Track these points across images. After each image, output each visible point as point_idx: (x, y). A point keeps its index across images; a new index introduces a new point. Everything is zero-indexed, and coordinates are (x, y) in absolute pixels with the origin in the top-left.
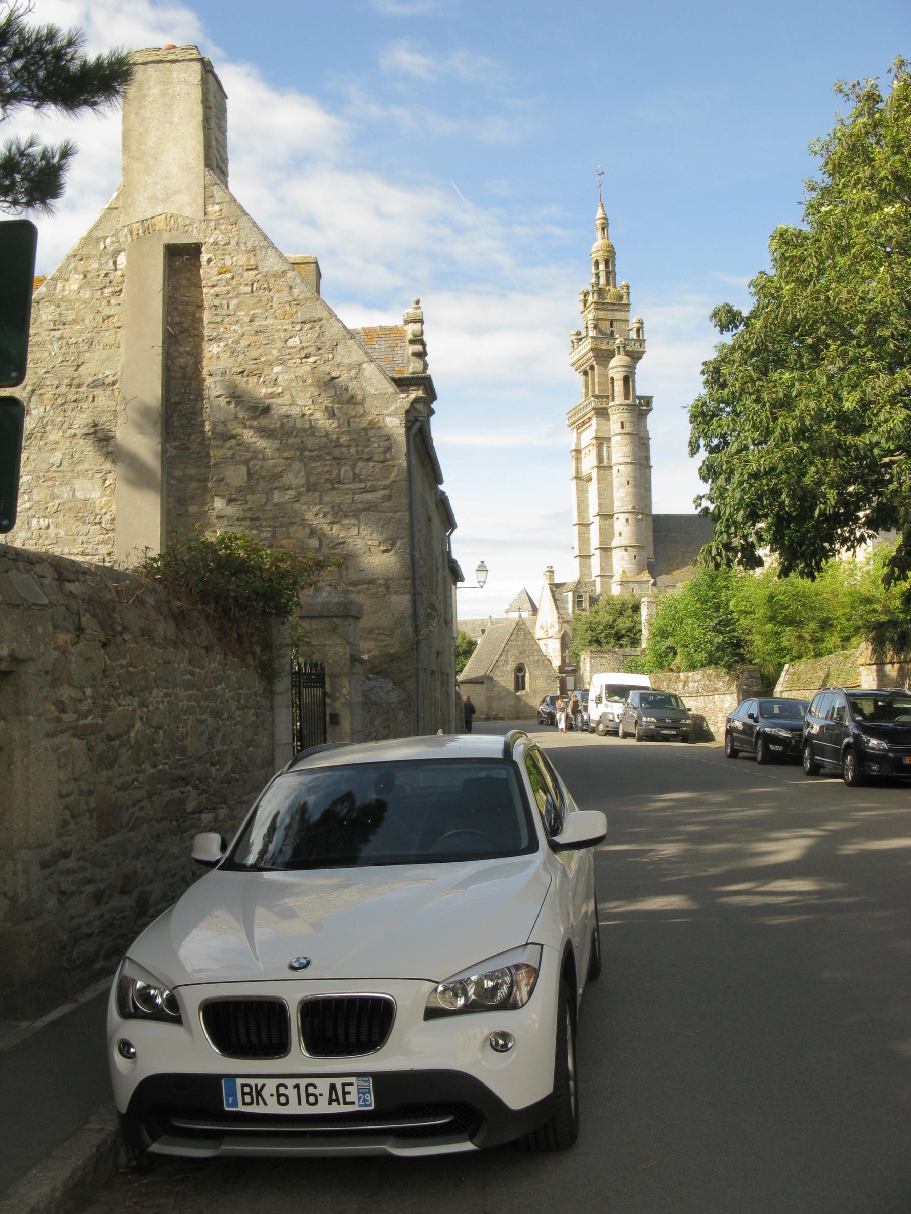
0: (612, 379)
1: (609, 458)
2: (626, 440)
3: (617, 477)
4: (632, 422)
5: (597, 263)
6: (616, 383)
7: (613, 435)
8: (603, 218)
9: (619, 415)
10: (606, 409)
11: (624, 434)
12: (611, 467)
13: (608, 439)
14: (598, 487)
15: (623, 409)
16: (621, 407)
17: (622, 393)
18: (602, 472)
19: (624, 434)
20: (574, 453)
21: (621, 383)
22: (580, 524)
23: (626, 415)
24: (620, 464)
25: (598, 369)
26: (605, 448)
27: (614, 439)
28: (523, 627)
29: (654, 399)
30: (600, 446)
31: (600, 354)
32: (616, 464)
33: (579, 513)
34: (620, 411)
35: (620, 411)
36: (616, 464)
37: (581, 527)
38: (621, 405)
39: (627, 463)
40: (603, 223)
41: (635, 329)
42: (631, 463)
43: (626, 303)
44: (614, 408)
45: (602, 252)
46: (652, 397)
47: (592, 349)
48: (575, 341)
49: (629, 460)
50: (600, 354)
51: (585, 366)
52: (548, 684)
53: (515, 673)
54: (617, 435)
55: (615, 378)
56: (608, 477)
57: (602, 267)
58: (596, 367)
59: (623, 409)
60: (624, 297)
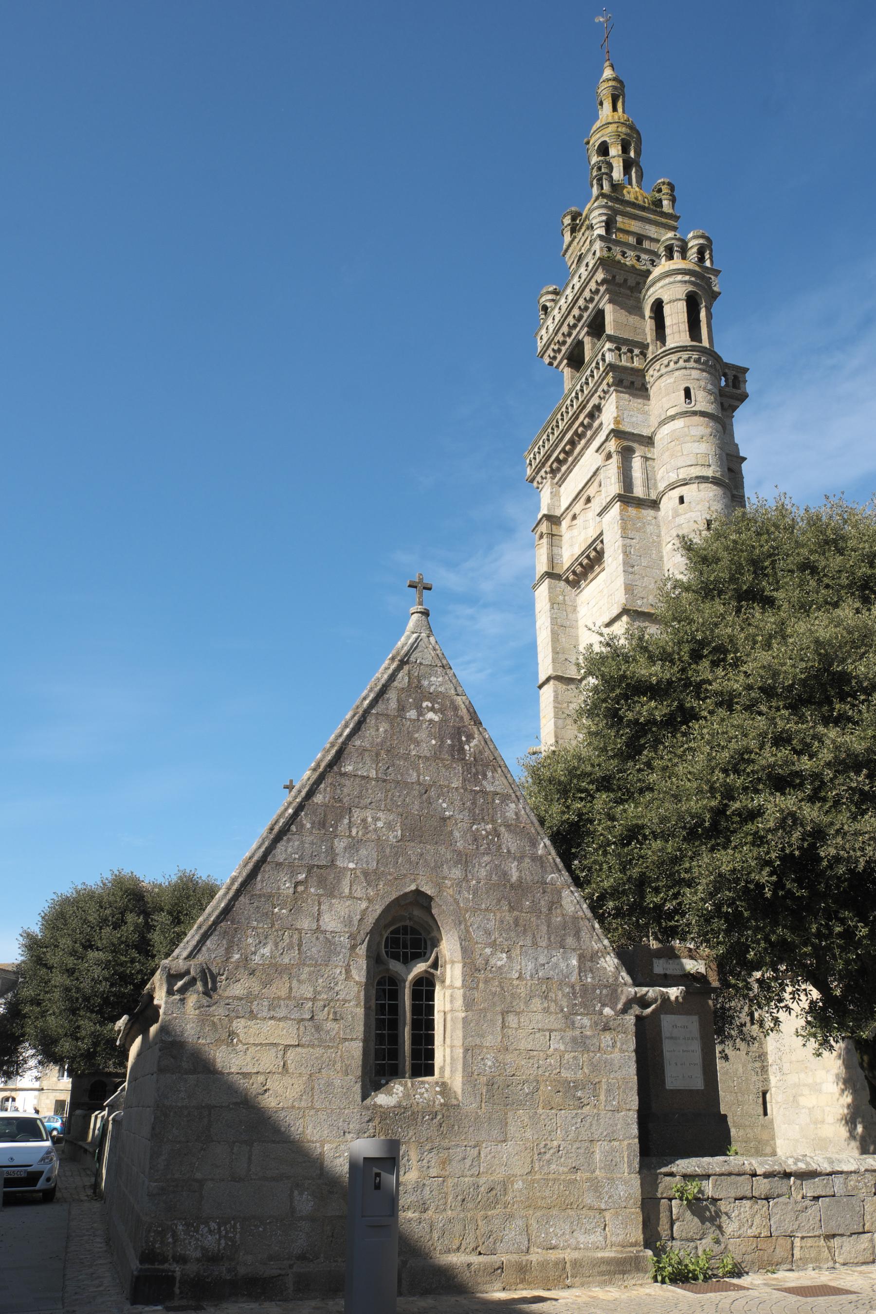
0: (658, 307)
1: (648, 481)
2: (701, 427)
3: (676, 515)
4: (710, 392)
5: (603, 149)
6: (667, 310)
7: (662, 423)
8: (615, 79)
9: (677, 373)
10: (641, 373)
11: (695, 413)
12: (654, 504)
13: (648, 441)
14: (624, 546)
15: (687, 360)
16: (685, 355)
17: (685, 327)
18: (632, 511)
19: (695, 413)
20: (544, 527)
21: (682, 306)
22: (559, 678)
23: (695, 374)
24: (685, 483)
25: (614, 311)
26: (637, 463)
27: (663, 436)
28: (435, 682)
29: (748, 376)
30: (626, 454)
31: (619, 279)
32: (672, 487)
33: (555, 652)
34: (681, 363)
35: (681, 363)
36: (672, 487)
37: (561, 687)
38: (683, 349)
39: (703, 479)
40: (614, 88)
41: (695, 250)
42: (715, 481)
43: (671, 211)
44: (665, 361)
45: (615, 125)
46: (745, 370)
47: (603, 262)
48: (548, 304)
49: (709, 473)
50: (619, 279)
51: (575, 333)
52: (581, 1043)
53: (375, 960)
54: (673, 418)
55: (665, 298)
56: (650, 529)
57: (615, 151)
58: (610, 311)
59: (687, 360)
60: (665, 203)
